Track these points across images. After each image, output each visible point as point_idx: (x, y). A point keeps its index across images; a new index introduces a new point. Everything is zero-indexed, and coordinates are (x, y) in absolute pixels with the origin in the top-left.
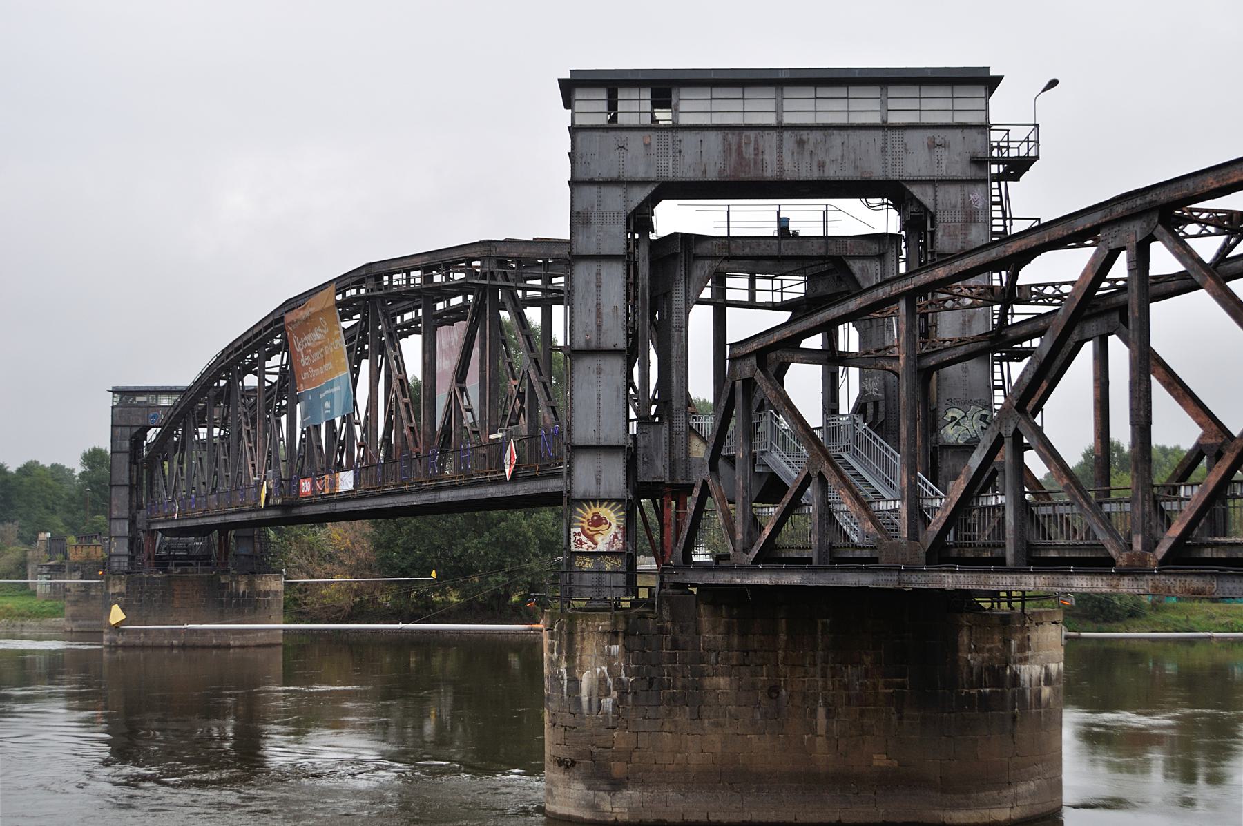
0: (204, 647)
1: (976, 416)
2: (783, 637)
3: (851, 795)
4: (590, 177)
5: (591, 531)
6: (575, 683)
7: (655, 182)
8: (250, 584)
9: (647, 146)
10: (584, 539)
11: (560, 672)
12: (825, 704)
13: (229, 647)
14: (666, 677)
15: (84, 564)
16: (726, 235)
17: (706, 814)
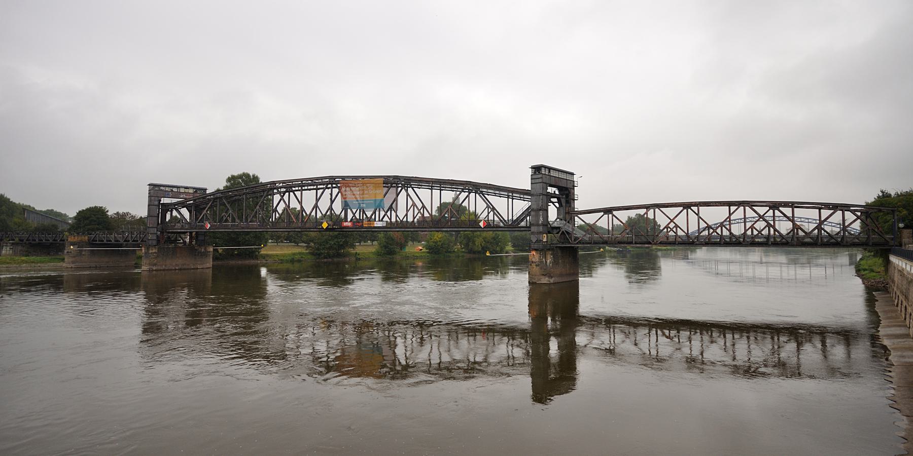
0: (188, 269)
6: (546, 262)
8: (205, 249)
13: (198, 269)
15: (79, 243)
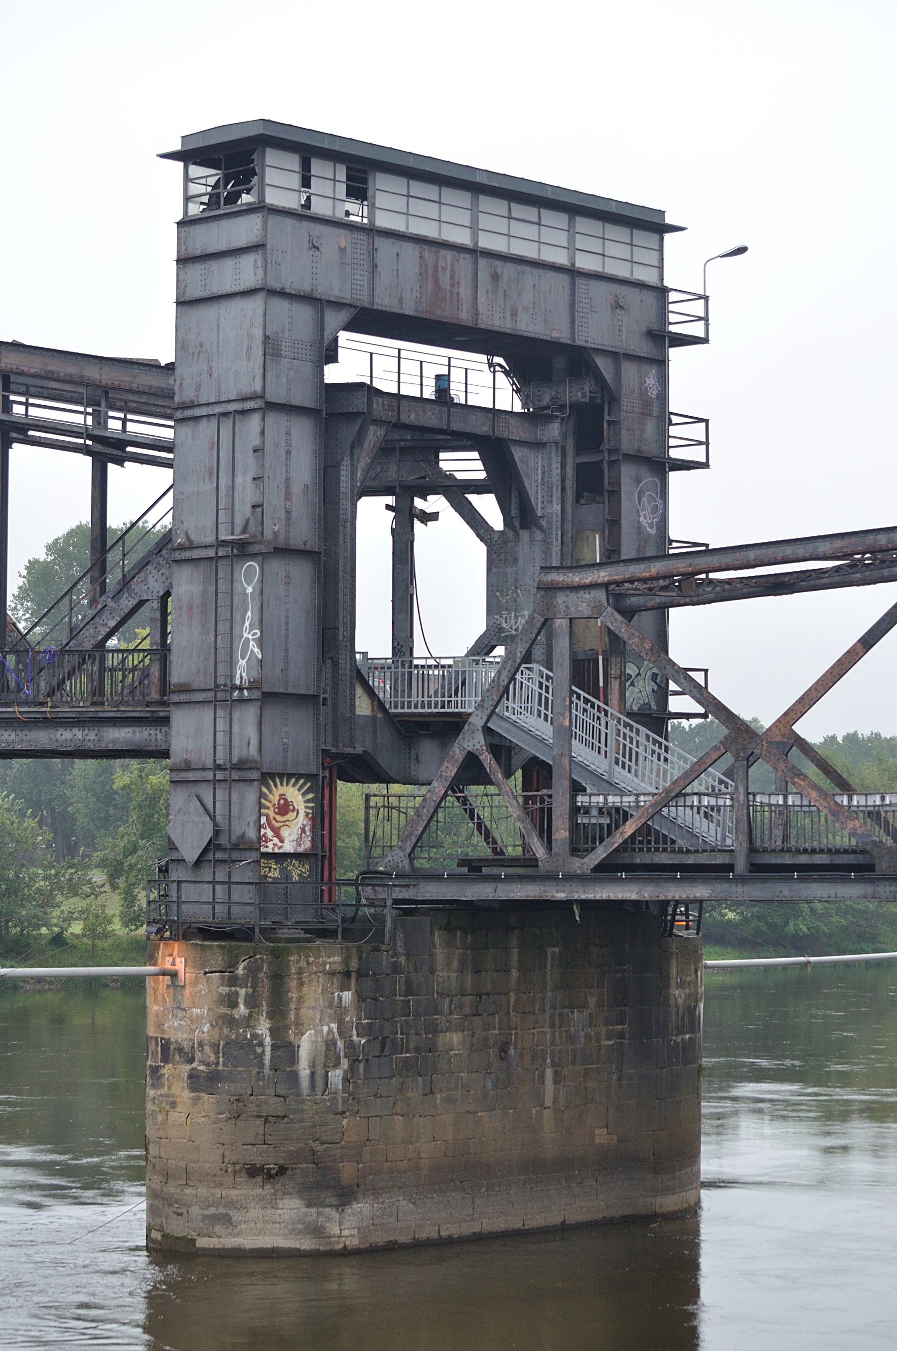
1: (648, 674)
2: (515, 973)
3: (575, 1185)
4: (281, 286)
5: (277, 821)
7: (351, 305)
9: (342, 250)
10: (270, 834)
11: (255, 1036)
12: (554, 1064)
14: (399, 1036)
16: (396, 392)
17: (437, 1228)
